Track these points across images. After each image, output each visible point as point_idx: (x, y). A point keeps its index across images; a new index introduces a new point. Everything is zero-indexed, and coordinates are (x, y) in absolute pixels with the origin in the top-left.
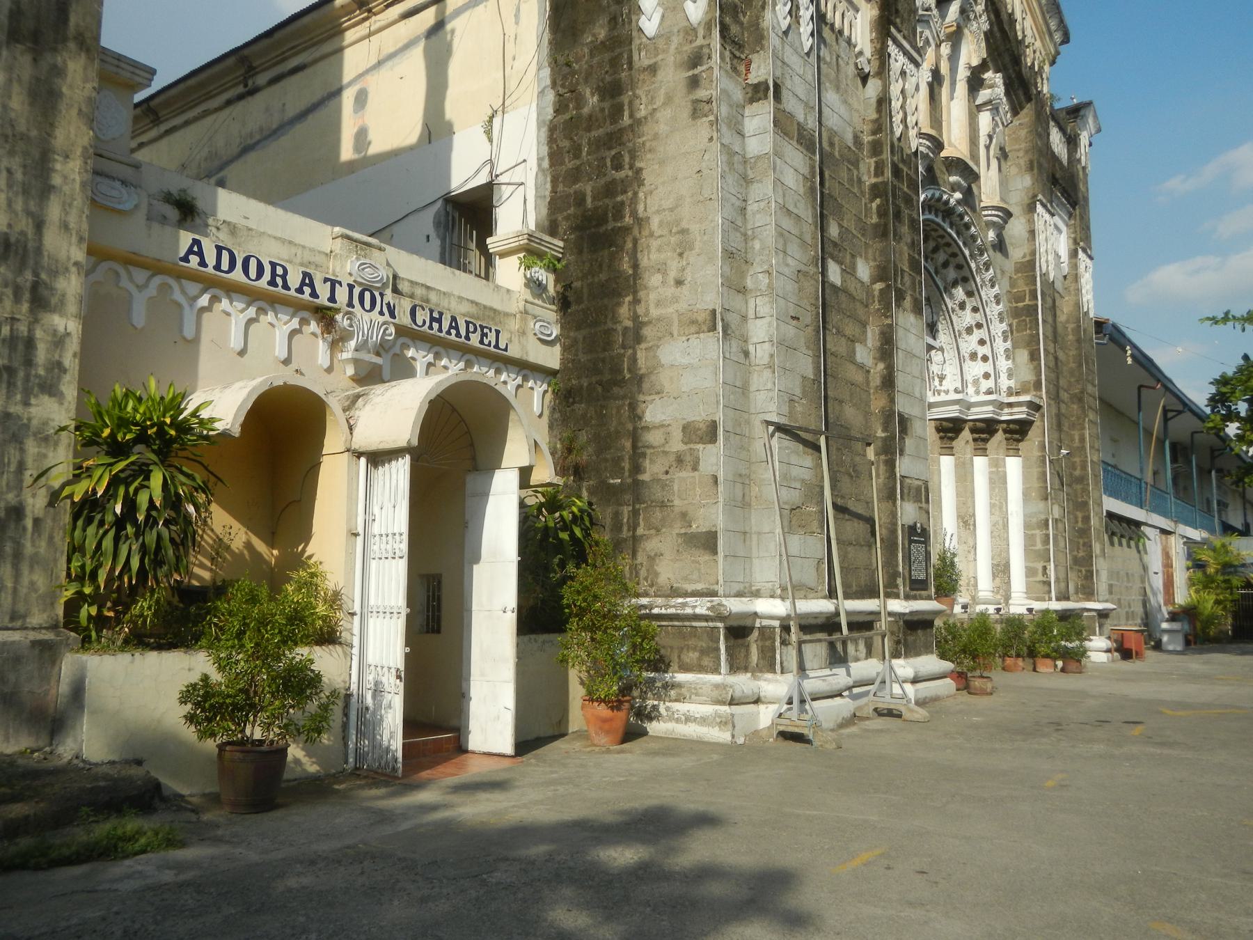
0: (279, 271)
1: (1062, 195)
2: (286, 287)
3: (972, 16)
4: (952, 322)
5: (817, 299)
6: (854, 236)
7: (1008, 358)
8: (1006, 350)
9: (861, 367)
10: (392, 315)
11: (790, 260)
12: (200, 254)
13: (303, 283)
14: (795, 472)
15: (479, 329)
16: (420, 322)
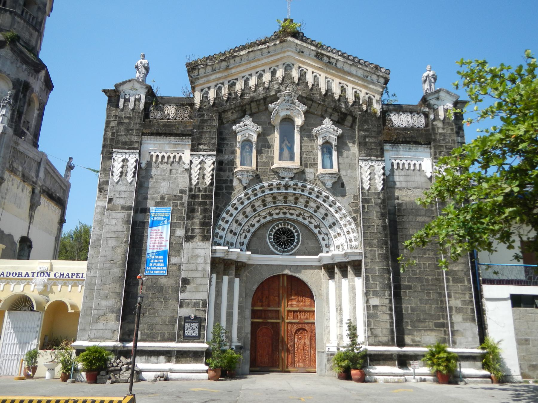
0: (20, 273)
1: (407, 144)
2: (21, 276)
3: (294, 109)
4: (323, 223)
5: (126, 252)
6: (175, 223)
7: (353, 232)
8: (352, 229)
9: (175, 265)
10: (49, 276)
11: (110, 245)
12: (3, 274)
13: (26, 275)
14: (103, 305)
15: (76, 275)
16: (57, 276)
